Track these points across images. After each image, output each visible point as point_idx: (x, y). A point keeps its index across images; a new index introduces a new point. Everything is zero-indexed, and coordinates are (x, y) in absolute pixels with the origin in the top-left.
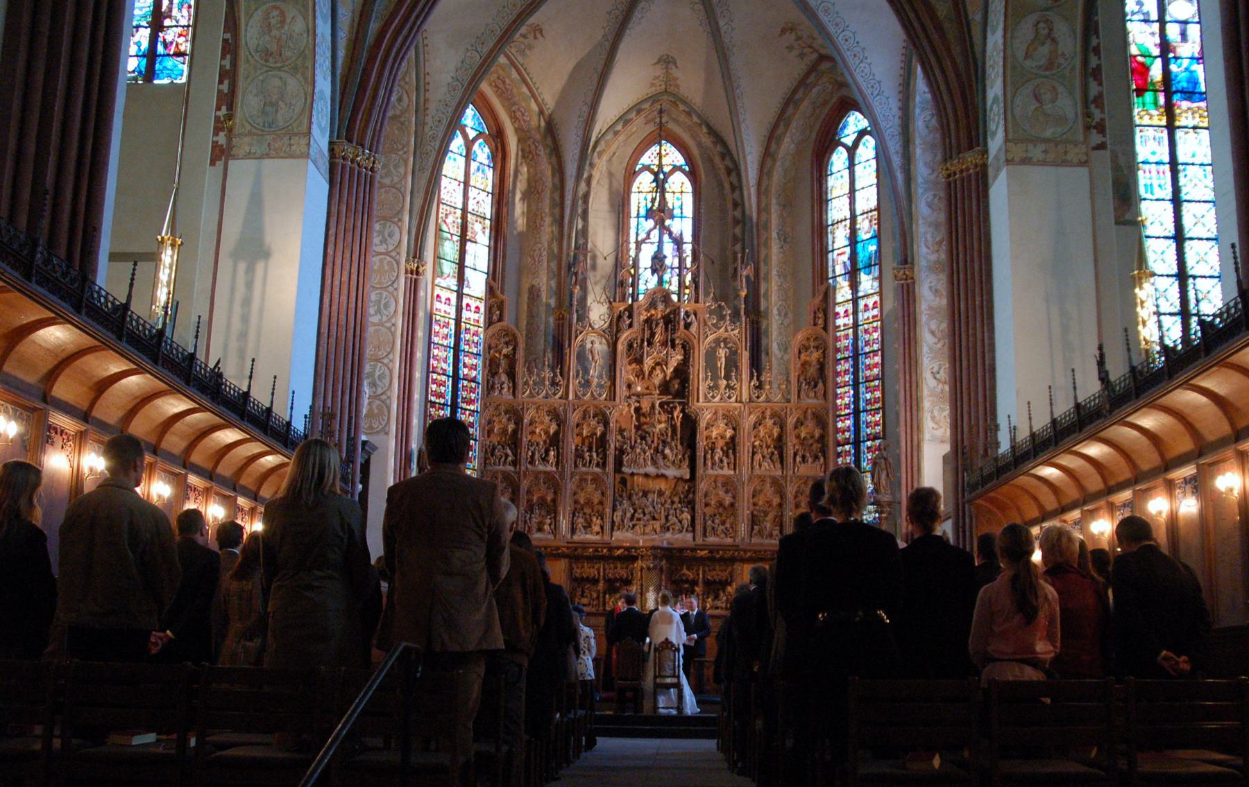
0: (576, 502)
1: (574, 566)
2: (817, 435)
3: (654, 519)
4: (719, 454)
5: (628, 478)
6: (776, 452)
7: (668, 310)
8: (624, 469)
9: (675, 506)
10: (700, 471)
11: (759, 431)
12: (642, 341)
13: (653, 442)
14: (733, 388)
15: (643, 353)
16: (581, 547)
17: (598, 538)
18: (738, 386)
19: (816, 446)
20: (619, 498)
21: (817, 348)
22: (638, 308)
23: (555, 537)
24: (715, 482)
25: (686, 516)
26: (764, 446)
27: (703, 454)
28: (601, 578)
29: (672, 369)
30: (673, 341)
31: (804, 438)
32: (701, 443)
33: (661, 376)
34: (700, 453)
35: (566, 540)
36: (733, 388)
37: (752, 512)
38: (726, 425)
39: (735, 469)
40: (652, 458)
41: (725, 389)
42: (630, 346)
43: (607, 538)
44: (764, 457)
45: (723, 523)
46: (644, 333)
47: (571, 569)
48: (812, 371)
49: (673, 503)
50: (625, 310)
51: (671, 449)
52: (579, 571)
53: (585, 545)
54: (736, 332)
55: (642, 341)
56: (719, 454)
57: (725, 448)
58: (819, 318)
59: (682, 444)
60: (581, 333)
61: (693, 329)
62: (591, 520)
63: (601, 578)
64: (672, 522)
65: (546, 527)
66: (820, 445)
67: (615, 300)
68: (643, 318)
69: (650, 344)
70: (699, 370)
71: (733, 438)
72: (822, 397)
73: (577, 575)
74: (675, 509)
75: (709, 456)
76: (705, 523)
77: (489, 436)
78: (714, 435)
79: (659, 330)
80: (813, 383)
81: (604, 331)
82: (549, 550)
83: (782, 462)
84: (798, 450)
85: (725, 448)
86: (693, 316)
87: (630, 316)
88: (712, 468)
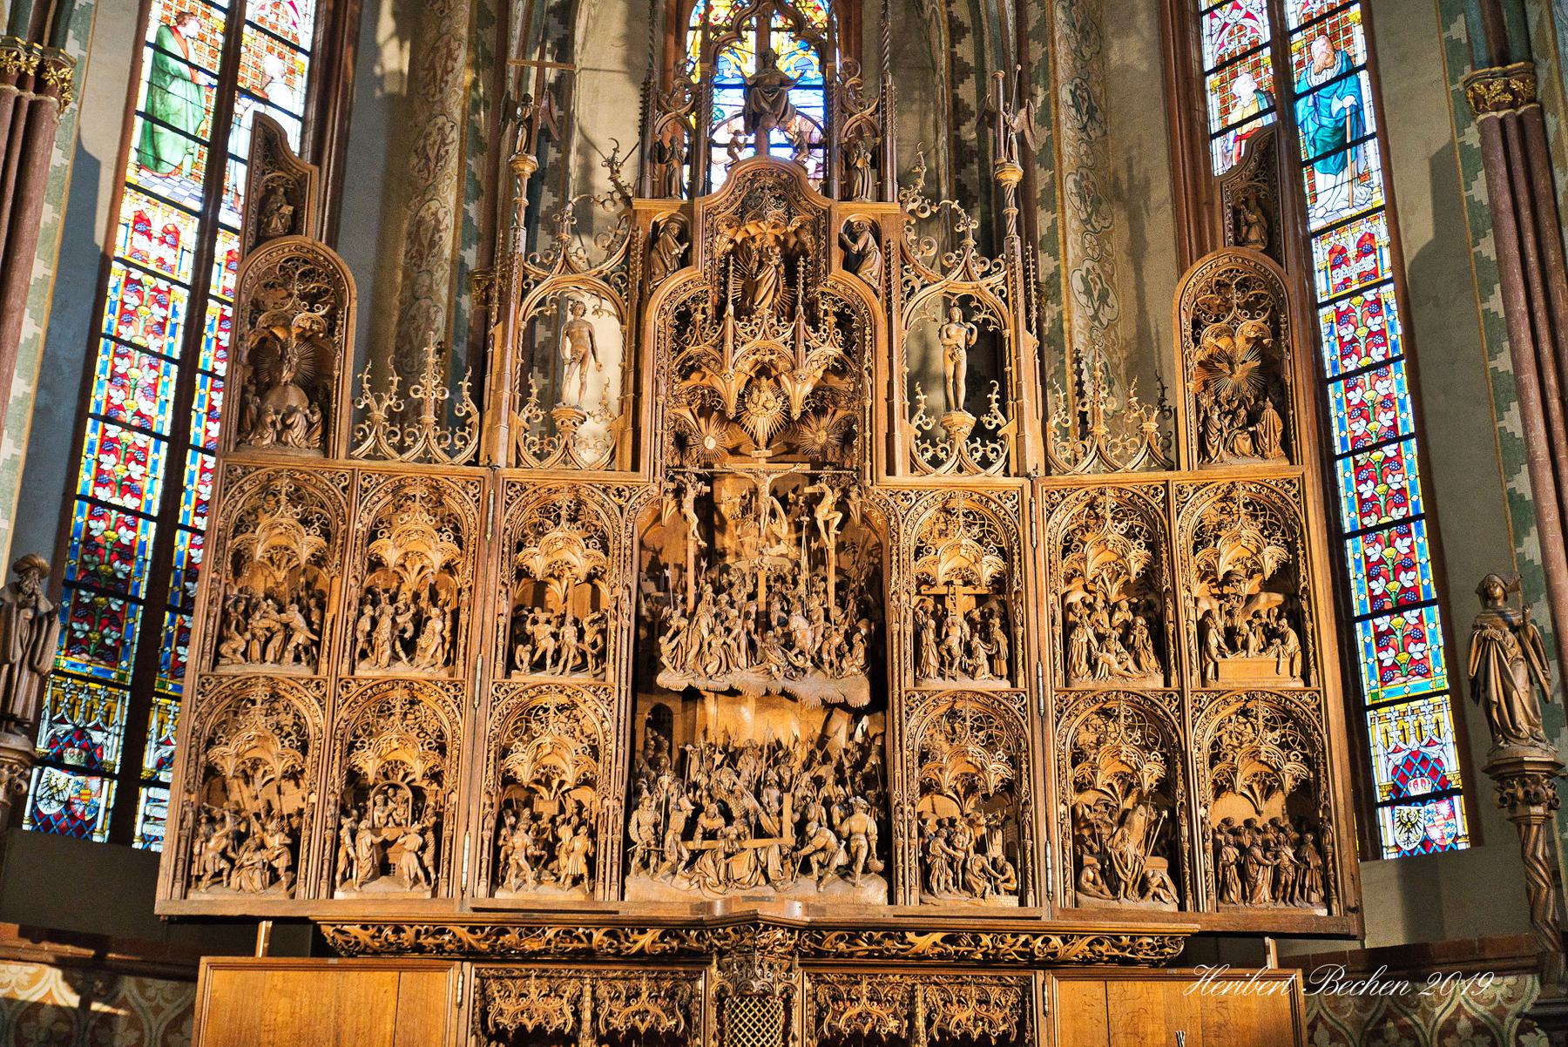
0: (508, 780)
1: (494, 987)
2: (1270, 566)
3: (760, 832)
4: (958, 632)
5: (675, 705)
6: (1140, 621)
7: (796, 222)
8: (663, 679)
9: (824, 792)
10: (903, 679)
11: (1085, 559)
12: (720, 309)
13: (752, 596)
14: (993, 436)
15: (723, 340)
16: (514, 924)
17: (574, 897)
18: (1009, 429)
19: (1269, 602)
20: (646, 768)
21: (1251, 308)
22: (707, 214)
23: (435, 893)
24: (952, 714)
25: (864, 823)
26: (1100, 604)
27: (910, 629)
28: (586, 1026)
29: (808, 389)
30: (811, 306)
31: (1228, 574)
32: (903, 601)
33: (776, 407)
34: (900, 628)
35: (469, 904)
36: (993, 436)
37: (1074, 810)
38: (979, 541)
39: (1012, 676)
40: (752, 645)
41: (972, 439)
42: (684, 318)
43: (606, 896)
44: (1101, 638)
45: (981, 847)
46: (725, 284)
47: (484, 998)
48: (1239, 377)
49: (818, 782)
50: (671, 219)
51: (808, 616)
52: (510, 1007)
53: (531, 921)
54: (996, 280)
55: (720, 309)
56: (958, 632)
57: (976, 614)
58: (1249, 225)
59: (842, 603)
60: (537, 283)
61: (873, 267)
62: (557, 839)
63: (586, 1026)
64: (818, 842)
65: (406, 863)
66: (1278, 598)
67: (640, 194)
68: (722, 245)
69: (744, 312)
70: (890, 385)
71: (1000, 583)
72: (1277, 449)
73: (505, 1021)
74: (827, 803)
75: (929, 636)
76: (925, 849)
77: (237, 572)
78: (941, 572)
79: (769, 277)
80: (1243, 412)
81: (606, 279)
82: (408, 935)
83: (1161, 654)
84: (1208, 613)
85: (976, 614)
86: (867, 239)
87: (682, 237)
88: (941, 674)
